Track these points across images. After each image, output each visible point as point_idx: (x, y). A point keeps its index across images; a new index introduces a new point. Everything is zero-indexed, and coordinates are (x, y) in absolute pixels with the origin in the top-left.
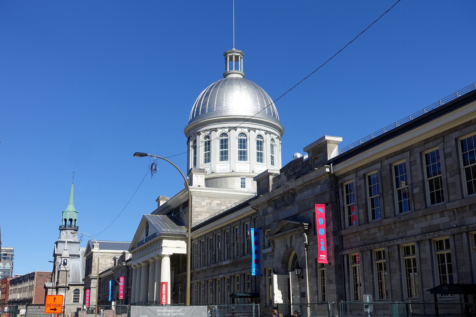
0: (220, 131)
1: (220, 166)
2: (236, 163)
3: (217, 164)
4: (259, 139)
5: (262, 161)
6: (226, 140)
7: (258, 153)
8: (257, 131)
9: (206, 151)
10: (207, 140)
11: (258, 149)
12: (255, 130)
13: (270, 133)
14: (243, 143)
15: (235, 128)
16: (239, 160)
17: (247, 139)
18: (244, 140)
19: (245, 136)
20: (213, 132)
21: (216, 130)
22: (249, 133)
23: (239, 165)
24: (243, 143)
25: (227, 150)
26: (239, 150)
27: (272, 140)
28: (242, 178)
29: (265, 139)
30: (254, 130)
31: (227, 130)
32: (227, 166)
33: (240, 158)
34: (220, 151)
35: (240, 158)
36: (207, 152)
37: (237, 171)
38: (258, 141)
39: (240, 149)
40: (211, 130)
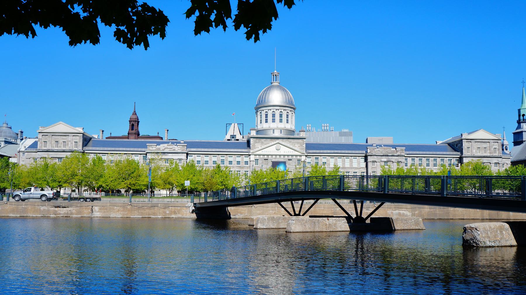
0: (265, 111)
4: (287, 114)
5: (282, 122)
9: (267, 119)
10: (261, 114)
11: (280, 117)
13: (292, 111)
14: (274, 115)
15: (271, 110)
20: (262, 111)
21: (263, 110)
24: (274, 115)
27: (292, 114)
33: (273, 122)
37: (279, 127)
38: (287, 115)
40: (262, 110)
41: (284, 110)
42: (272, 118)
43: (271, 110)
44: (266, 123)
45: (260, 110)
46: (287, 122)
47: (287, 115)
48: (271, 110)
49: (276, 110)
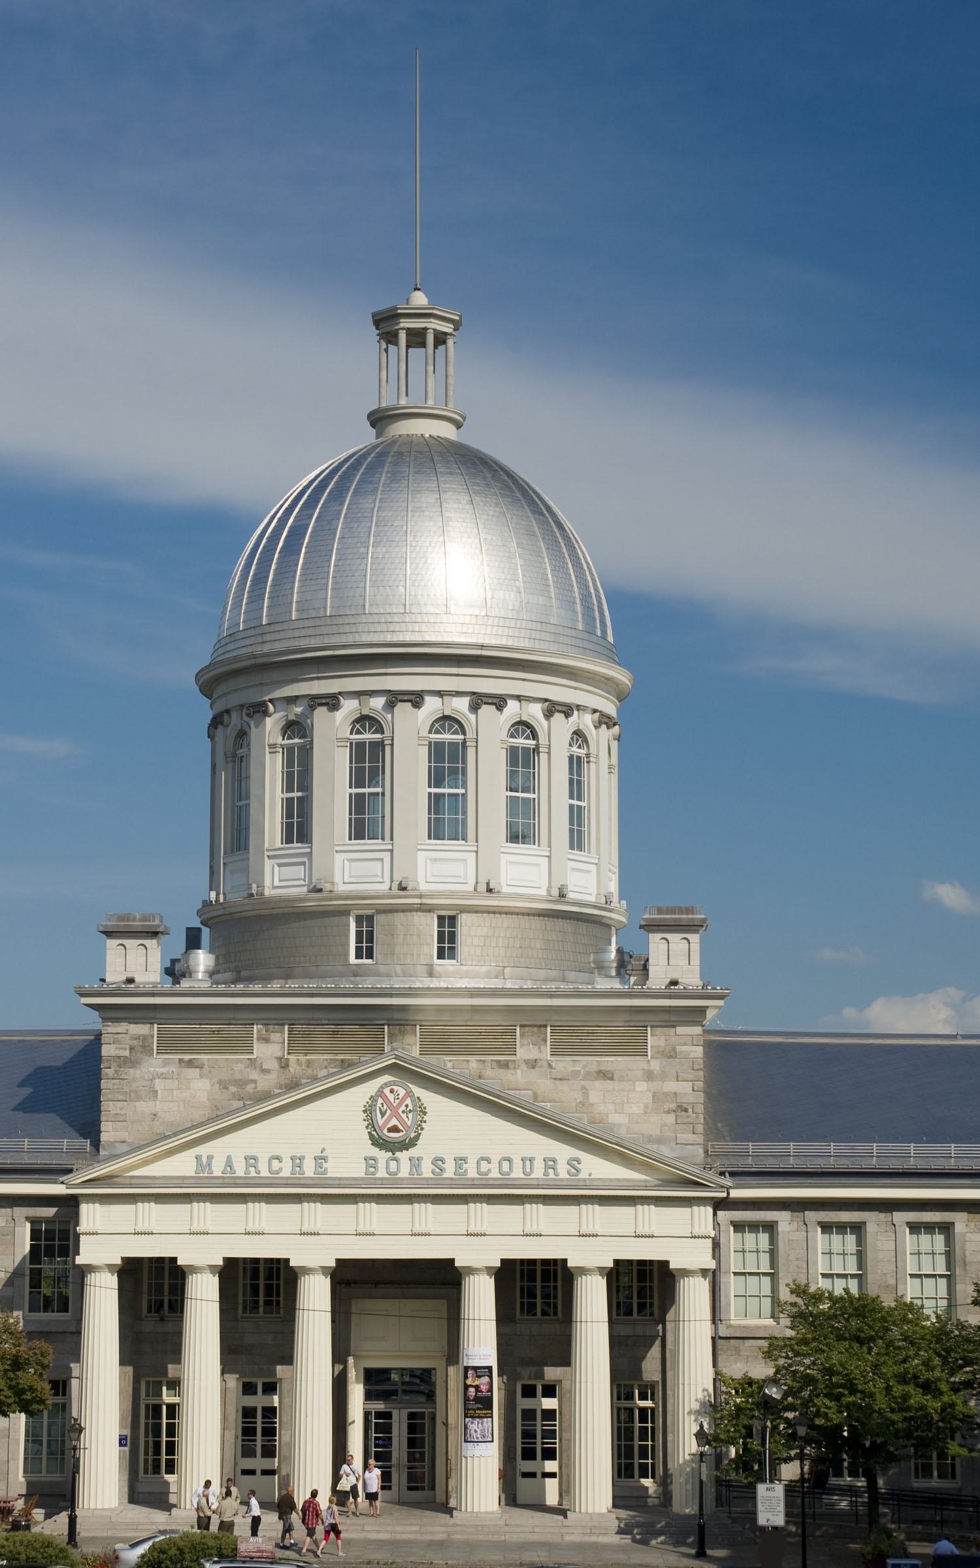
1: (350, 860)
2: (419, 850)
3: (337, 855)
6: (378, 746)
7: (512, 803)
8: (512, 706)
12: (499, 702)
16: (429, 838)
17: (468, 744)
18: (454, 746)
19: (456, 733)
22: (473, 717)
23: (435, 860)
25: (379, 790)
26: (430, 794)
28: (441, 919)
29: (543, 740)
30: (495, 704)
31: (378, 703)
32: (379, 864)
34: (351, 795)
35: (436, 831)
36: (296, 794)
39: (434, 790)
40: (315, 701)
41: (474, 708)
42: (424, 790)
43: (499, 702)
44: (289, 840)
45: (292, 700)
46: (577, 840)
47: (576, 764)
48: (500, 708)
49: (478, 701)
